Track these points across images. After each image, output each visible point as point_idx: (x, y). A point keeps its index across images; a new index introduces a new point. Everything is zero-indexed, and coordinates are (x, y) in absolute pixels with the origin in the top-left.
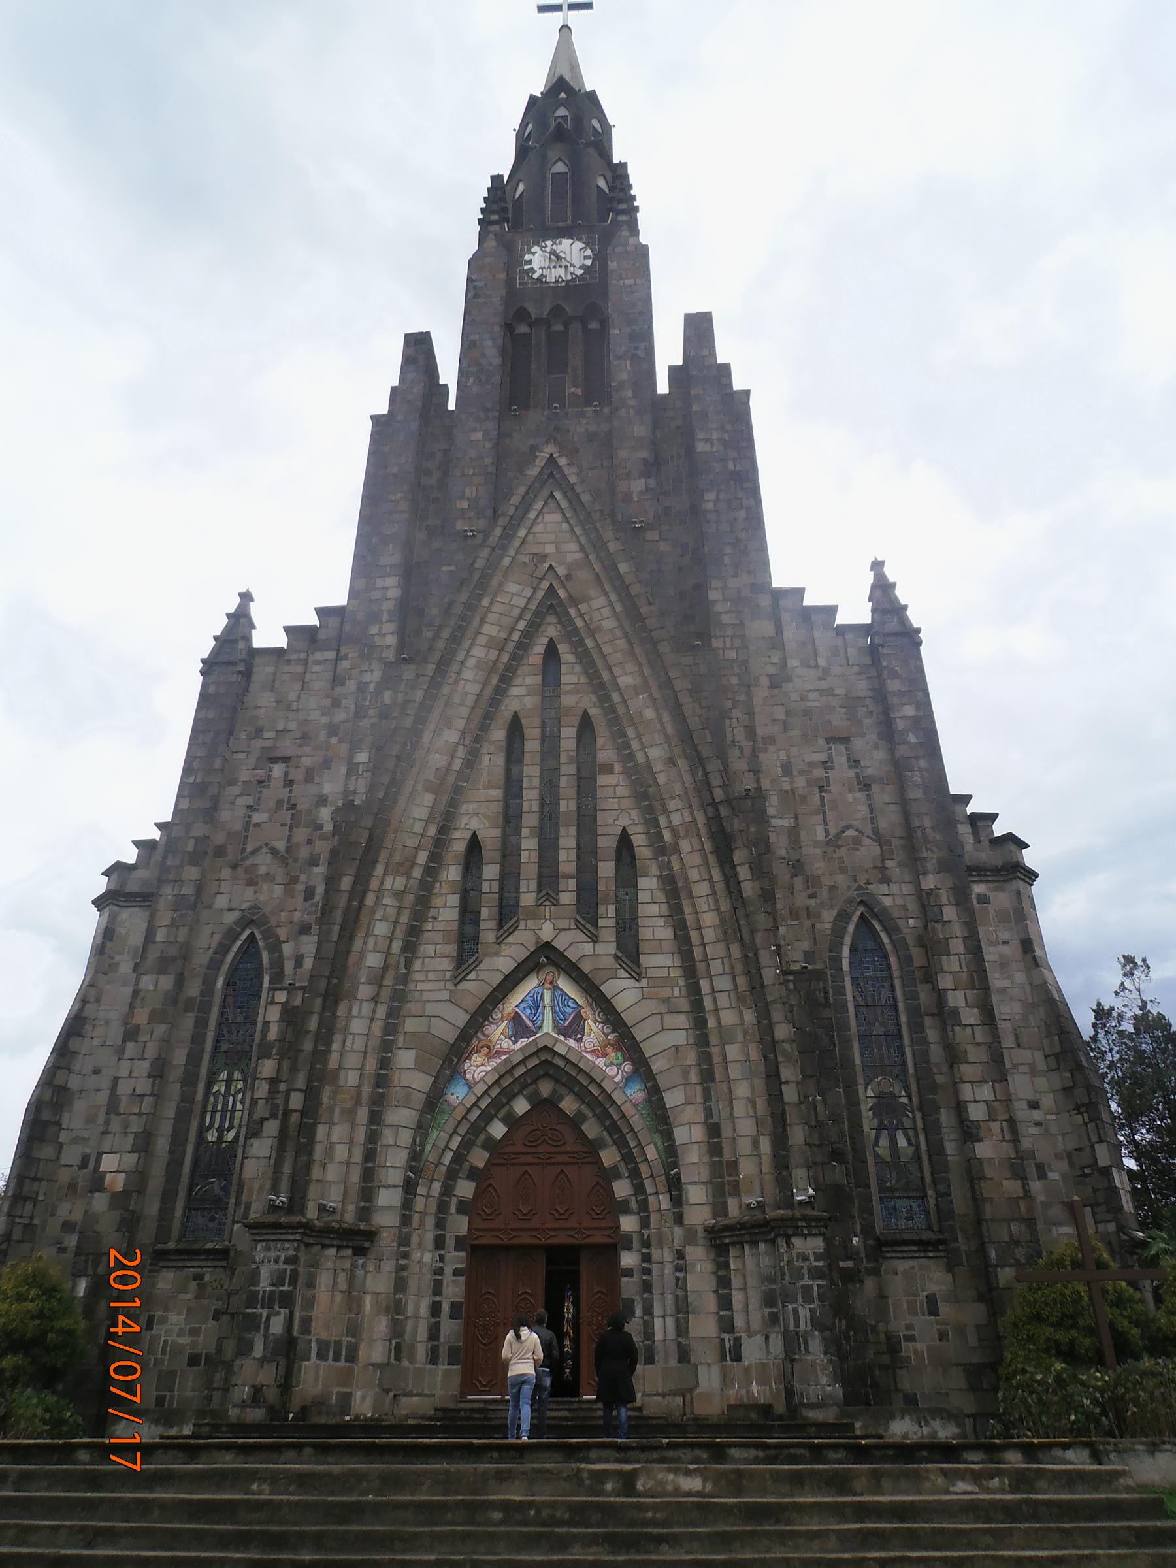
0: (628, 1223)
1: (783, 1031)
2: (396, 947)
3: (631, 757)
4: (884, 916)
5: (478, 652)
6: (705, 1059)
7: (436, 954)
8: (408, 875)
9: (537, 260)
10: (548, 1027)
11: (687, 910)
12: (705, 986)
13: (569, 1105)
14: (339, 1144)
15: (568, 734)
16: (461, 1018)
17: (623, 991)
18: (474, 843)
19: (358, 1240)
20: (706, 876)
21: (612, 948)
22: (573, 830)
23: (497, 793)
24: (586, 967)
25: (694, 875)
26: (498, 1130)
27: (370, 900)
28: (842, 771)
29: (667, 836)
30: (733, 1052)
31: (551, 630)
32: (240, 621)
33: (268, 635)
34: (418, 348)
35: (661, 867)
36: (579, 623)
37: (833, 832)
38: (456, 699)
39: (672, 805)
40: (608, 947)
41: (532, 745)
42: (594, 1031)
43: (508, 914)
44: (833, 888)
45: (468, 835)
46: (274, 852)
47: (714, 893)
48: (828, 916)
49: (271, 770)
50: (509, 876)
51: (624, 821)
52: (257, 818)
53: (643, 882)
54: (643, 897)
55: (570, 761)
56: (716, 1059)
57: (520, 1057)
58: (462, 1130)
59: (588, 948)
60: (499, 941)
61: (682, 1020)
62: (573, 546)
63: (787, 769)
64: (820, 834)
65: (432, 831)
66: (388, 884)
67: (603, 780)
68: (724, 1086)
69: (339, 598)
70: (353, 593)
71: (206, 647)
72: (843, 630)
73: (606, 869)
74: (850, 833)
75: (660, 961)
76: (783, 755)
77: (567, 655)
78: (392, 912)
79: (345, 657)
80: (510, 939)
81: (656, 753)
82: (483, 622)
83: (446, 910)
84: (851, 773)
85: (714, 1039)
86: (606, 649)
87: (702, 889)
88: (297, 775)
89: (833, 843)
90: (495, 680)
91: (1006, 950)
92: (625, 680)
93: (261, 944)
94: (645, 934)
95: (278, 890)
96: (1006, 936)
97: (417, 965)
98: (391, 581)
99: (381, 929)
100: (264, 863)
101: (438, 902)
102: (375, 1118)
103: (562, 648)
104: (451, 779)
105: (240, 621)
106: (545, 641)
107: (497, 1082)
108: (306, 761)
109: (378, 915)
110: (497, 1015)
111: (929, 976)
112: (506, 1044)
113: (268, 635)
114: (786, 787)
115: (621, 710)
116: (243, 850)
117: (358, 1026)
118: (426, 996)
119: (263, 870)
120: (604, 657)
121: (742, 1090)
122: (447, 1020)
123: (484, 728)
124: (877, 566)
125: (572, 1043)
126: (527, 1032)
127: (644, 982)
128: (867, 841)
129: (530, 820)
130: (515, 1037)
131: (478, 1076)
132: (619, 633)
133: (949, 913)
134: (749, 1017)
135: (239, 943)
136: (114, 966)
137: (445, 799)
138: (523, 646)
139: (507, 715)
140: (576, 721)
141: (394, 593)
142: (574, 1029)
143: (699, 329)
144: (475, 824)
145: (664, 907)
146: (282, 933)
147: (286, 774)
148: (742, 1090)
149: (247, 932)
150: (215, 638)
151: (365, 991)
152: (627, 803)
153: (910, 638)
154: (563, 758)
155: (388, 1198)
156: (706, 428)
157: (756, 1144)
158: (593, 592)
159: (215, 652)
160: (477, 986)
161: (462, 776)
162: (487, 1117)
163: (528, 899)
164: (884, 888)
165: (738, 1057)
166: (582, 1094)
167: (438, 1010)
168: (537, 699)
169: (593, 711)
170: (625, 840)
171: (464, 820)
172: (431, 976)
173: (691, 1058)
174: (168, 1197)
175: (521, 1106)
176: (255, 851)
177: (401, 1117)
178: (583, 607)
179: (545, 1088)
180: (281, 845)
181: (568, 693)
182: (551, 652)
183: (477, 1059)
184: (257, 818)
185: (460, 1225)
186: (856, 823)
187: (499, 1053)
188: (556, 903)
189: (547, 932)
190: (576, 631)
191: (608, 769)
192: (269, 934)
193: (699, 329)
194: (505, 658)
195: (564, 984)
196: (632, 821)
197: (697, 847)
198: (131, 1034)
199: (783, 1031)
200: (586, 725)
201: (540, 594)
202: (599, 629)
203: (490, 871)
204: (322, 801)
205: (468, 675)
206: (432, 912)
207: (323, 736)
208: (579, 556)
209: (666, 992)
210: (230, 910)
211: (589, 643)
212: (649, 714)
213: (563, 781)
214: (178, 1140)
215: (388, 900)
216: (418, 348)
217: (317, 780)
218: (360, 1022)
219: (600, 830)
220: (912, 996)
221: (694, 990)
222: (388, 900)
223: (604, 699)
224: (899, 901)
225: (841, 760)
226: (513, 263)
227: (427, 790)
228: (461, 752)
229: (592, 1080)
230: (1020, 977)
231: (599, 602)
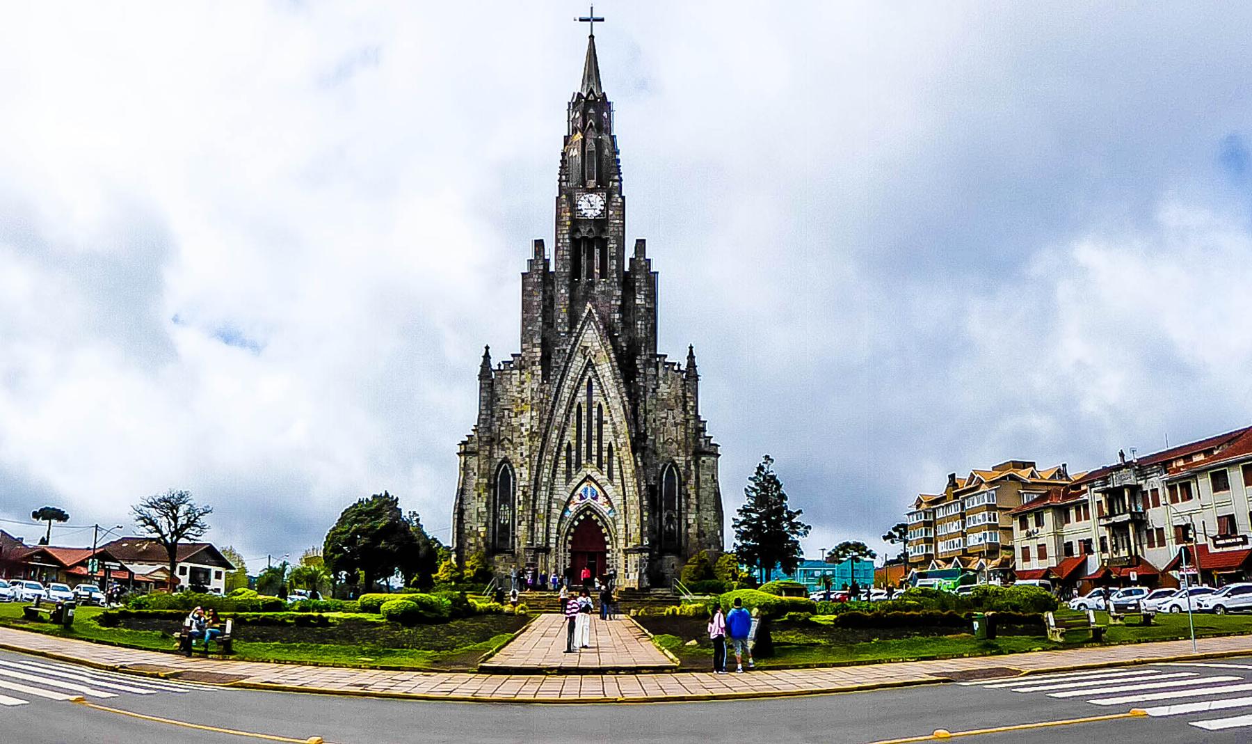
0: (607, 539)
1: (645, 503)
4: (676, 466)
7: (561, 477)
9: (583, 204)
13: (594, 517)
14: (540, 527)
15: (595, 410)
17: (609, 489)
18: (569, 444)
19: (547, 550)
26: (576, 523)
31: (590, 373)
32: (487, 357)
34: (539, 244)
41: (584, 413)
42: (601, 499)
43: (579, 465)
73: (605, 454)
75: (617, 481)
83: (563, 465)
88: (512, 415)
89: (664, 443)
98: (538, 350)
102: (548, 521)
105: (487, 357)
122: (564, 496)
124: (691, 348)
129: (584, 438)
133: (693, 467)
138: (582, 380)
141: (539, 354)
142: (596, 498)
143: (641, 244)
153: (696, 377)
155: (552, 540)
156: (638, 281)
159: (482, 371)
163: (584, 462)
165: (634, 508)
167: (562, 493)
174: (494, 537)
175: (582, 517)
177: (554, 521)
182: (590, 381)
185: (569, 546)
192: (511, 465)
193: (641, 244)
195: (594, 485)
196: (612, 439)
198: (479, 495)
199: (645, 503)
203: (574, 453)
204: (522, 425)
212: (617, 406)
214: (494, 523)
216: (539, 244)
218: (543, 496)
225: (670, 417)
226: (573, 207)
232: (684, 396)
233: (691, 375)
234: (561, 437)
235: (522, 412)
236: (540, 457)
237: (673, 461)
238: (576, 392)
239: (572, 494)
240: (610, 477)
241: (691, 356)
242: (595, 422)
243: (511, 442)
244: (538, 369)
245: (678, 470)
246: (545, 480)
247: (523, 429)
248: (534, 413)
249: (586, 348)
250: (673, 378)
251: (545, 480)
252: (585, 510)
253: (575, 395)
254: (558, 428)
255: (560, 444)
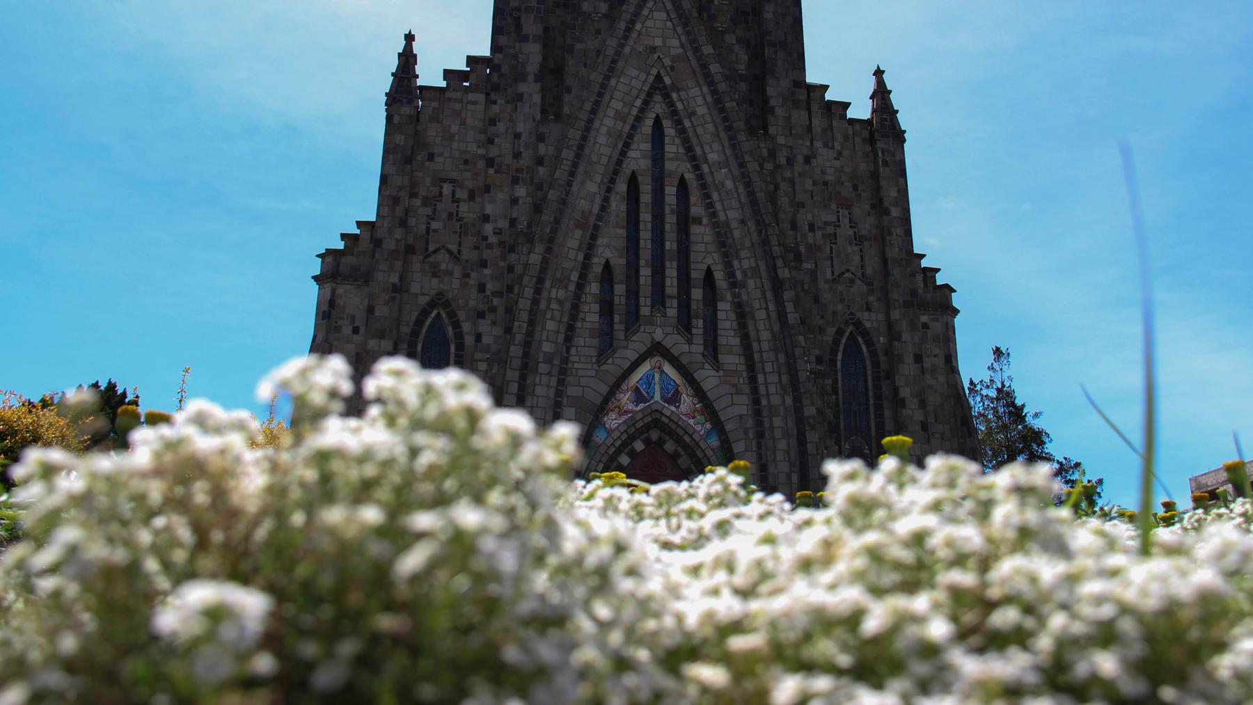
2: (561, 338)
3: (714, 215)
4: (865, 333)
5: (608, 122)
6: (759, 423)
7: (586, 344)
8: (566, 287)
10: (657, 397)
11: (751, 328)
12: (760, 378)
13: (670, 446)
15: (671, 191)
16: (604, 389)
17: (709, 378)
18: (607, 265)
20: (764, 306)
21: (701, 349)
22: (675, 264)
23: (623, 232)
24: (684, 361)
25: (756, 304)
27: (543, 305)
28: (845, 231)
29: (739, 275)
30: (777, 422)
31: (658, 107)
32: (407, 59)
33: (429, 75)
35: (735, 296)
36: (679, 106)
37: (837, 273)
38: (594, 159)
39: (743, 254)
40: (698, 348)
41: (646, 198)
42: (687, 401)
43: (633, 319)
44: (835, 313)
45: (603, 261)
46: (449, 251)
47: (769, 317)
48: (831, 331)
49: (441, 187)
50: (633, 294)
51: (709, 261)
52: (435, 225)
53: (721, 305)
54: (721, 315)
55: (672, 212)
56: (767, 425)
57: (640, 416)
58: (604, 460)
59: (685, 348)
60: (627, 339)
61: (744, 399)
62: (675, 42)
63: (812, 227)
64: (829, 275)
65: (581, 257)
66: (553, 295)
67: (694, 229)
68: (771, 443)
69: (484, 50)
70: (495, 47)
71: (386, 83)
72: (853, 122)
73: (697, 294)
74: (848, 275)
75: (732, 360)
76: (809, 217)
77: (669, 131)
78: (557, 314)
79: (495, 102)
80: (634, 338)
81: (733, 215)
82: (611, 98)
83: (591, 315)
84: (851, 232)
85: (765, 413)
86: (700, 130)
87: (761, 315)
90: (620, 146)
91: (935, 360)
92: (713, 157)
93: (446, 321)
94: (722, 341)
95: (456, 283)
96: (936, 351)
97: (573, 351)
99: (551, 325)
100: (443, 259)
101: (585, 308)
103: (666, 123)
104: (592, 220)
105: (407, 59)
106: (654, 116)
107: (626, 431)
108: (469, 184)
109: (549, 316)
110: (624, 387)
111: (890, 376)
112: (631, 407)
113: (429, 75)
114: (811, 241)
115: (709, 179)
116: (427, 250)
117: (539, 390)
118: (580, 373)
119: (443, 266)
120: (697, 136)
121: (782, 445)
123: (613, 181)
124: (879, 73)
125: (673, 408)
126: (645, 400)
127: (721, 373)
128: (858, 282)
130: (637, 402)
131: (614, 426)
132: (708, 118)
134: (789, 401)
135: (430, 320)
136: (338, 329)
137: (588, 235)
138: (638, 119)
139: (628, 173)
140: (676, 182)
142: (674, 399)
144: (608, 253)
145: (735, 324)
146: (462, 315)
147: (454, 192)
148: (782, 445)
149: (435, 312)
150: (393, 74)
151: (543, 368)
152: (711, 248)
154: (667, 210)
157: (789, 477)
158: (691, 83)
160: (613, 367)
161: (599, 218)
162: (618, 452)
163: (645, 311)
164: (866, 315)
166: (678, 440)
168: (649, 162)
169: (687, 176)
170: (709, 273)
171: (600, 250)
172: (583, 359)
173: (750, 423)
175: (639, 446)
176: (435, 252)
178: (683, 94)
179: (655, 435)
180: (454, 248)
181: (670, 159)
182: (658, 123)
183: (613, 415)
184: (435, 225)
186: (852, 269)
187: (626, 412)
188: (665, 315)
189: (658, 335)
190: (675, 112)
191: (698, 221)
192: (452, 314)
194: (627, 129)
195: (668, 369)
197: (759, 285)
200: (682, 184)
201: (651, 79)
202: (693, 114)
203: (620, 289)
204: (486, 218)
205: (602, 140)
206: (581, 315)
207: (481, 164)
208: (680, 51)
209: (735, 380)
210: (423, 294)
211: (687, 123)
212: (729, 184)
213: (667, 227)
215: (554, 306)
217: (478, 199)
219: (693, 266)
220: (877, 387)
221: (753, 380)
222: (554, 306)
223: (697, 168)
224: (875, 325)
225: (845, 221)
227: (576, 227)
228: (598, 200)
229: (686, 432)
230: (942, 379)
231: (695, 91)
232: (875, 176)
233: (885, 128)
234: (589, 248)
235: (487, 189)
236: (538, 291)
237: (858, 324)
238: (627, 145)
239: (616, 387)
240: (712, 349)
241: (881, 94)
242: (671, 220)
243: (456, 257)
244: (532, 91)
245: (870, 343)
246: (547, 347)
247: (488, 228)
248: (521, 191)
249: (654, 49)
250: (846, 137)
251: (547, 347)
252: (647, 427)
253: (623, 153)
254: (580, 225)
255: (586, 266)
